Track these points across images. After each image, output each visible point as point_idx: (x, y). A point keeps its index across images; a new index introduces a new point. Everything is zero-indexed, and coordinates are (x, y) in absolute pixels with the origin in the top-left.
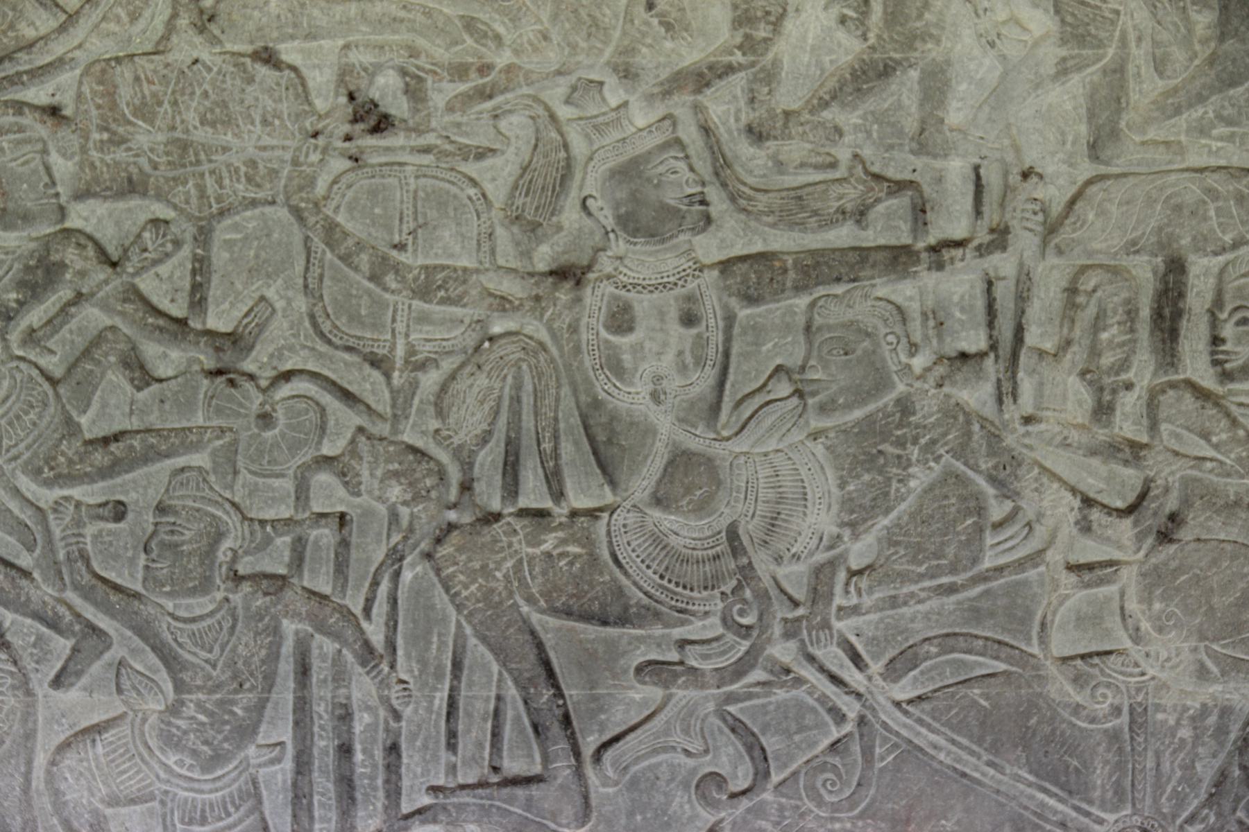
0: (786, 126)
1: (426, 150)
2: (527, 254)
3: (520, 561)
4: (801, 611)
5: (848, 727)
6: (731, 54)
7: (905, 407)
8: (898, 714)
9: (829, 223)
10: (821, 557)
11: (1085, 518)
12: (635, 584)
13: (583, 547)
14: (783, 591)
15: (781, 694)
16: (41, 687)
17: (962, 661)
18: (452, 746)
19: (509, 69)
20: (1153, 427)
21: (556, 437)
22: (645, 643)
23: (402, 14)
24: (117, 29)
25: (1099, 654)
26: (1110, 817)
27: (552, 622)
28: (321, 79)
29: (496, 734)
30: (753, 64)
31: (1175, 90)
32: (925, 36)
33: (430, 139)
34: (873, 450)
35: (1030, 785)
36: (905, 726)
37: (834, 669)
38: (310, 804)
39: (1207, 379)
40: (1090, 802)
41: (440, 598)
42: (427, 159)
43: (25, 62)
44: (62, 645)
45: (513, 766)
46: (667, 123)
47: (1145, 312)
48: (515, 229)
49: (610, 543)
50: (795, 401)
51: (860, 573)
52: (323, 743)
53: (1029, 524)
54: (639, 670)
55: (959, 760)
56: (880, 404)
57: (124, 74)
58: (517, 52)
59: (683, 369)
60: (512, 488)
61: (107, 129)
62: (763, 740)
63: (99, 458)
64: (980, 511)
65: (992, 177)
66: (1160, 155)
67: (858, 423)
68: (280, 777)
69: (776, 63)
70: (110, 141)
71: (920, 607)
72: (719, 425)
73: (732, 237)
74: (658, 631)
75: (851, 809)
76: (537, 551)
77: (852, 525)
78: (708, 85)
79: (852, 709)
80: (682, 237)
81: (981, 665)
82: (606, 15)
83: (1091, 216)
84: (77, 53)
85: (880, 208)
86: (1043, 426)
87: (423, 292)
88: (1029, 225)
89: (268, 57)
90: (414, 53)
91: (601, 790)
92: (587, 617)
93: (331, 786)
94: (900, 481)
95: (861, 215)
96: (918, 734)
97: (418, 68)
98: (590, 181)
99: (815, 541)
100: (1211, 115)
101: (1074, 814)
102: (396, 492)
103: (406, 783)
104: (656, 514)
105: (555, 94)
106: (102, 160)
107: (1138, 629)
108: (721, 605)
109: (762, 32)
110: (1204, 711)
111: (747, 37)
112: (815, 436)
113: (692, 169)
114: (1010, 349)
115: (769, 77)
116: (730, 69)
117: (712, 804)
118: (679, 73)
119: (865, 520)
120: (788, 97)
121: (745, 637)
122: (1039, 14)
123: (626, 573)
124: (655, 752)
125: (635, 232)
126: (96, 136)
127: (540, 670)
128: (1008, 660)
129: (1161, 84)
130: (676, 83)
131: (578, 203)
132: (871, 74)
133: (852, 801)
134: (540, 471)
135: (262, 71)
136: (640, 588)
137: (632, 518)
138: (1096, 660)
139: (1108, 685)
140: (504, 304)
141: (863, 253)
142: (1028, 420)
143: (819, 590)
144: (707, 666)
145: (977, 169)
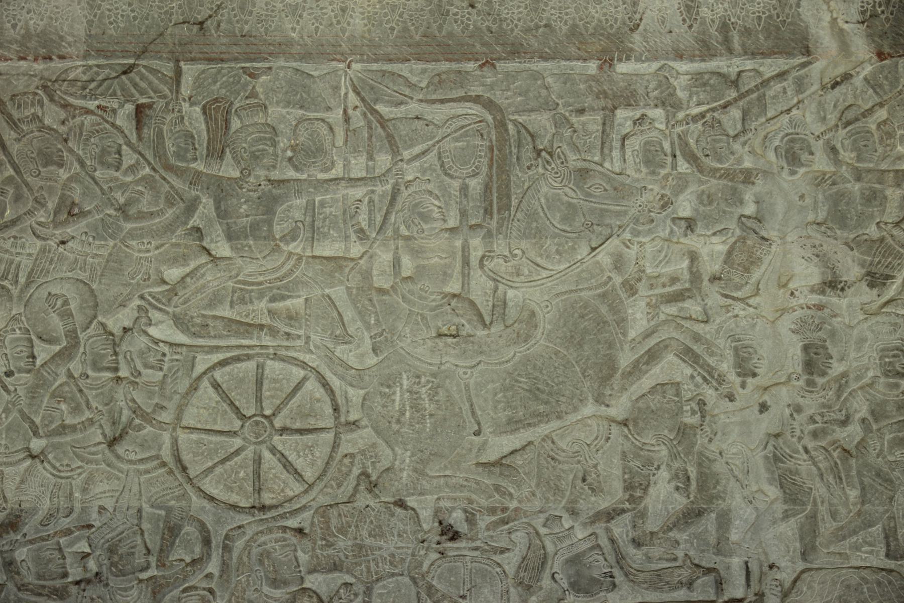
0: (651, 539)
1: (476, 549)
6: (624, 504)
9: (675, 588)
19: (516, 510)
23: (465, 483)
24: (331, 491)
28: (426, 514)
30: (634, 509)
31: (842, 528)
32: (718, 497)
33: (478, 543)
42: (477, 553)
43: (288, 507)
46: (593, 537)
48: (520, 589)
57: (334, 512)
58: (520, 502)
61: (325, 539)
65: (754, 567)
66: (837, 560)
69: (646, 508)
70: (326, 545)
78: (613, 518)
80: (602, 594)
82: (563, 484)
83: (805, 589)
84: (312, 503)
85: (699, 581)
88: (774, 592)
89: (401, 504)
90: (471, 501)
95: (690, 585)
97: (473, 509)
98: (556, 565)
100: (861, 540)
105: (538, 522)
106: (322, 554)
111: (631, 495)
113: (606, 560)
115: (643, 515)
116: (623, 511)
118: (598, 512)
120: (652, 525)
122: (773, 488)
125: (578, 591)
126: (320, 543)
129: (834, 524)
130: (597, 517)
131: (550, 576)
132: (692, 515)
135: (399, 510)
145: (746, 563)
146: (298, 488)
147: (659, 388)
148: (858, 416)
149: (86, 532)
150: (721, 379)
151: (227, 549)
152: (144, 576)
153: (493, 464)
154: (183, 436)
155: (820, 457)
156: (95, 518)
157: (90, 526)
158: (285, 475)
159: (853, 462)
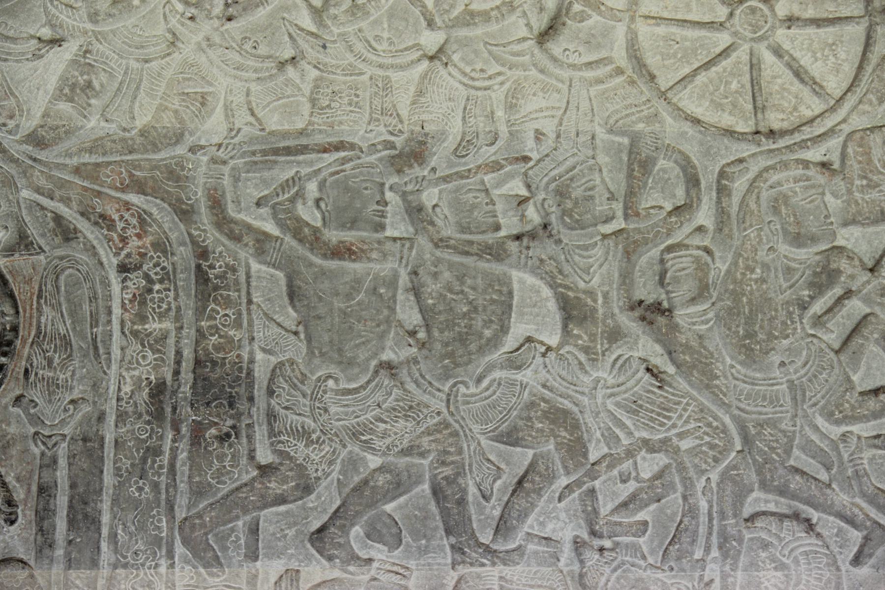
16: (845, 566)
24: (870, 109)
43: (808, 132)
44: (856, 536)
61: (865, 178)
63: (872, 404)
70: (868, 186)
84: (843, 126)
106: (863, 199)
126: (858, 182)
146: (813, 106)
149: (521, 167)
151: (722, 191)
152: (608, 229)
154: (644, 29)
156: (530, 147)
157: (526, 159)
158: (797, 86)
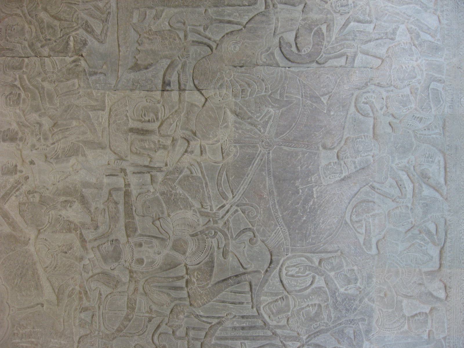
0: (95, 221)
1: (99, 307)
2: (124, 284)
3: (199, 287)
4: (211, 220)
5: (239, 209)
6: (77, 233)
7: (163, 194)
8: (236, 197)
9: (118, 211)
10: (198, 215)
11: (190, 152)
12: (204, 259)
13: (195, 271)
14: (206, 224)
15: (231, 225)
17: (223, 182)
18: (243, 303)
19: (80, 287)
20: (169, 136)
21: (169, 278)
22: (218, 257)
23: (67, 312)
25: (222, 150)
26: (260, 149)
27: (213, 279)
29: (240, 293)
30: (80, 228)
31: (90, 130)
33: (97, 306)
34: (172, 201)
35: (252, 167)
36: (238, 196)
37: (225, 212)
38: (255, 336)
39: (157, 124)
40: (256, 153)
41: (207, 305)
42: (101, 307)
45: (248, 289)
46: (93, 249)
47: (142, 137)
48: (118, 286)
49: (194, 265)
50: (161, 220)
51: (202, 206)
52: (241, 333)
53: (191, 165)
54: (225, 258)
55: (247, 183)
56: (162, 200)
58: (76, 285)
59: (152, 247)
60: (181, 288)
62: (242, 229)
64: (188, 176)
65: (109, 172)
67: (166, 205)
68: (249, 343)
69: (80, 223)
71: (210, 191)
72: (166, 238)
73: (121, 235)
74: (215, 254)
75: (258, 209)
76: (196, 283)
77: (191, 207)
78: (85, 239)
79: (234, 208)
80: (121, 246)
81: (224, 177)
83: (119, 149)
85: (115, 198)
86: (168, 161)
87: (133, 309)
88: (120, 163)
91: (253, 267)
92: (212, 271)
93: (251, 331)
94: (180, 195)
95: (116, 203)
96: (240, 193)
97: (80, 309)
98: (107, 268)
99: (194, 216)
100: (96, 122)
101: (259, 157)
102: (181, 316)
103: (251, 314)
104: (187, 254)
105: (86, 276)
107: (216, 141)
108: (210, 239)
109: (73, 226)
110: (235, 127)
111: (74, 230)
112: (169, 215)
113: (104, 243)
114: (149, 168)
115: (83, 224)
116: (81, 234)
117: (257, 241)
118: (82, 246)
119: (190, 204)
120: (88, 220)
121: (217, 233)
122: (71, 161)
123: (202, 261)
124: (244, 255)
125: (120, 258)
127: (225, 282)
128: (223, 171)
129: (89, 133)
130: (84, 247)
131: (112, 271)
132: (83, 200)
133: (256, 209)
134: (177, 281)
136: (205, 258)
137: (188, 260)
138: (223, 151)
139: (229, 148)
140: (136, 290)
141: (126, 203)
142: (166, 165)
143: (207, 215)
144: (224, 242)
145: (106, 176)
147: (21, 213)
148: (38, 118)
150: (18, 182)
153: (58, 297)
155: (56, 137)
159: (59, 122)
